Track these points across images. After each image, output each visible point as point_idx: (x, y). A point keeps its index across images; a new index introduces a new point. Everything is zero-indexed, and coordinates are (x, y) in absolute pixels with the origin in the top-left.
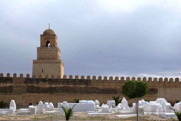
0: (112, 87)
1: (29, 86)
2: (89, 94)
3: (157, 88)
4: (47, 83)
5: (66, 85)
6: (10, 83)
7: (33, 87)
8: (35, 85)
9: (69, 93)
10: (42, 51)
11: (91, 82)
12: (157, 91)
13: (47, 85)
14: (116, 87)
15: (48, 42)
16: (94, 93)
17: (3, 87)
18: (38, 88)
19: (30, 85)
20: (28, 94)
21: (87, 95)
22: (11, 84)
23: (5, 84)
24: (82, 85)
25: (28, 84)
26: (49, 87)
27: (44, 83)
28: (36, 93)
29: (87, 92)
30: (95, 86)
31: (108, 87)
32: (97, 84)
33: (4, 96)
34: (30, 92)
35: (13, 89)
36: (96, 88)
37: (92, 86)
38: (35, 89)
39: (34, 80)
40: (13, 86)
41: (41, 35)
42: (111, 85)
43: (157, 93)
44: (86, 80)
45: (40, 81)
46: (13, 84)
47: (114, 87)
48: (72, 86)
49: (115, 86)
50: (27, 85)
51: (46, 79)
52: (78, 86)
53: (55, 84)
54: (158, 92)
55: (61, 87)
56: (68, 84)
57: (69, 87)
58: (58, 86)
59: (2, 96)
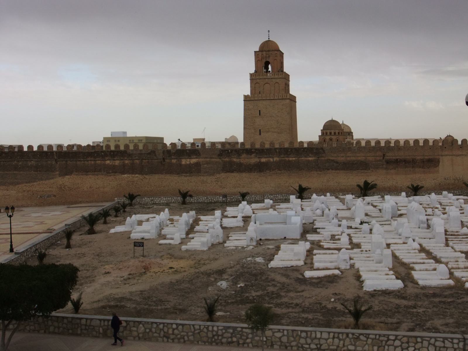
0: (359, 158)
2: (321, 171)
3: (438, 157)
4: (253, 155)
5: (284, 159)
6: (197, 158)
8: (235, 160)
9: (289, 170)
10: (258, 80)
11: (324, 151)
12: (438, 161)
13: (253, 160)
15: (267, 64)
16: (331, 170)
17: (186, 165)
18: (240, 165)
19: (227, 159)
20: (223, 175)
21: (318, 172)
22: (198, 159)
23: (188, 160)
24: (310, 157)
25: (224, 159)
26: (256, 162)
27: (249, 156)
28: (237, 172)
31: (354, 158)
33: (188, 178)
34: (227, 172)
35: (202, 166)
37: (326, 158)
38: (235, 166)
39: (233, 152)
40: (201, 163)
41: (255, 52)
42: (358, 155)
46: (201, 160)
47: (364, 158)
48: (294, 159)
49: (364, 157)
50: (222, 161)
51: (252, 149)
52: (303, 158)
53: (265, 158)
54: (440, 164)
56: (287, 157)
57: (289, 161)
58: (271, 160)
59: (185, 178)
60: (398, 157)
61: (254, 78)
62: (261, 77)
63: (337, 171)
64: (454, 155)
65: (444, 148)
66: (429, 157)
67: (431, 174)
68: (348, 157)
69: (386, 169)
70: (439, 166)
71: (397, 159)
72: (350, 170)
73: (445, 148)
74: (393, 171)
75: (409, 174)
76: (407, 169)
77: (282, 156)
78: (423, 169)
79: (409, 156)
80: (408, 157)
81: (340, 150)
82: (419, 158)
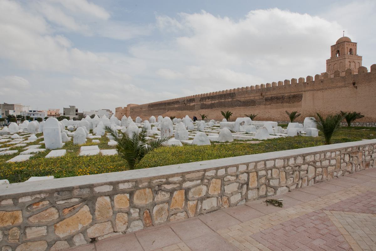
1: (201, 104)
2: (233, 107)
3: (301, 93)
7: (203, 104)
8: (204, 103)
14: (254, 98)
18: (206, 105)
19: (202, 103)
29: (233, 105)
30: (238, 99)
31: (248, 98)
32: (240, 97)
36: (239, 100)
39: (204, 99)
43: (301, 101)
44: (232, 93)
45: (206, 99)
47: (253, 97)
48: (223, 100)
55: (217, 103)
57: (222, 102)
60: (273, 96)
61: (328, 62)
62: (332, 61)
63: (240, 107)
64: (315, 90)
65: (307, 85)
66: (295, 93)
67: (295, 108)
68: (246, 97)
69: (265, 105)
70: (302, 101)
71: (272, 97)
72: (246, 106)
73: (308, 84)
74: (269, 106)
75: (279, 109)
76: (278, 104)
77: (219, 99)
78: (289, 104)
79: (280, 94)
80: (279, 95)
81: (242, 93)
82: (287, 95)
